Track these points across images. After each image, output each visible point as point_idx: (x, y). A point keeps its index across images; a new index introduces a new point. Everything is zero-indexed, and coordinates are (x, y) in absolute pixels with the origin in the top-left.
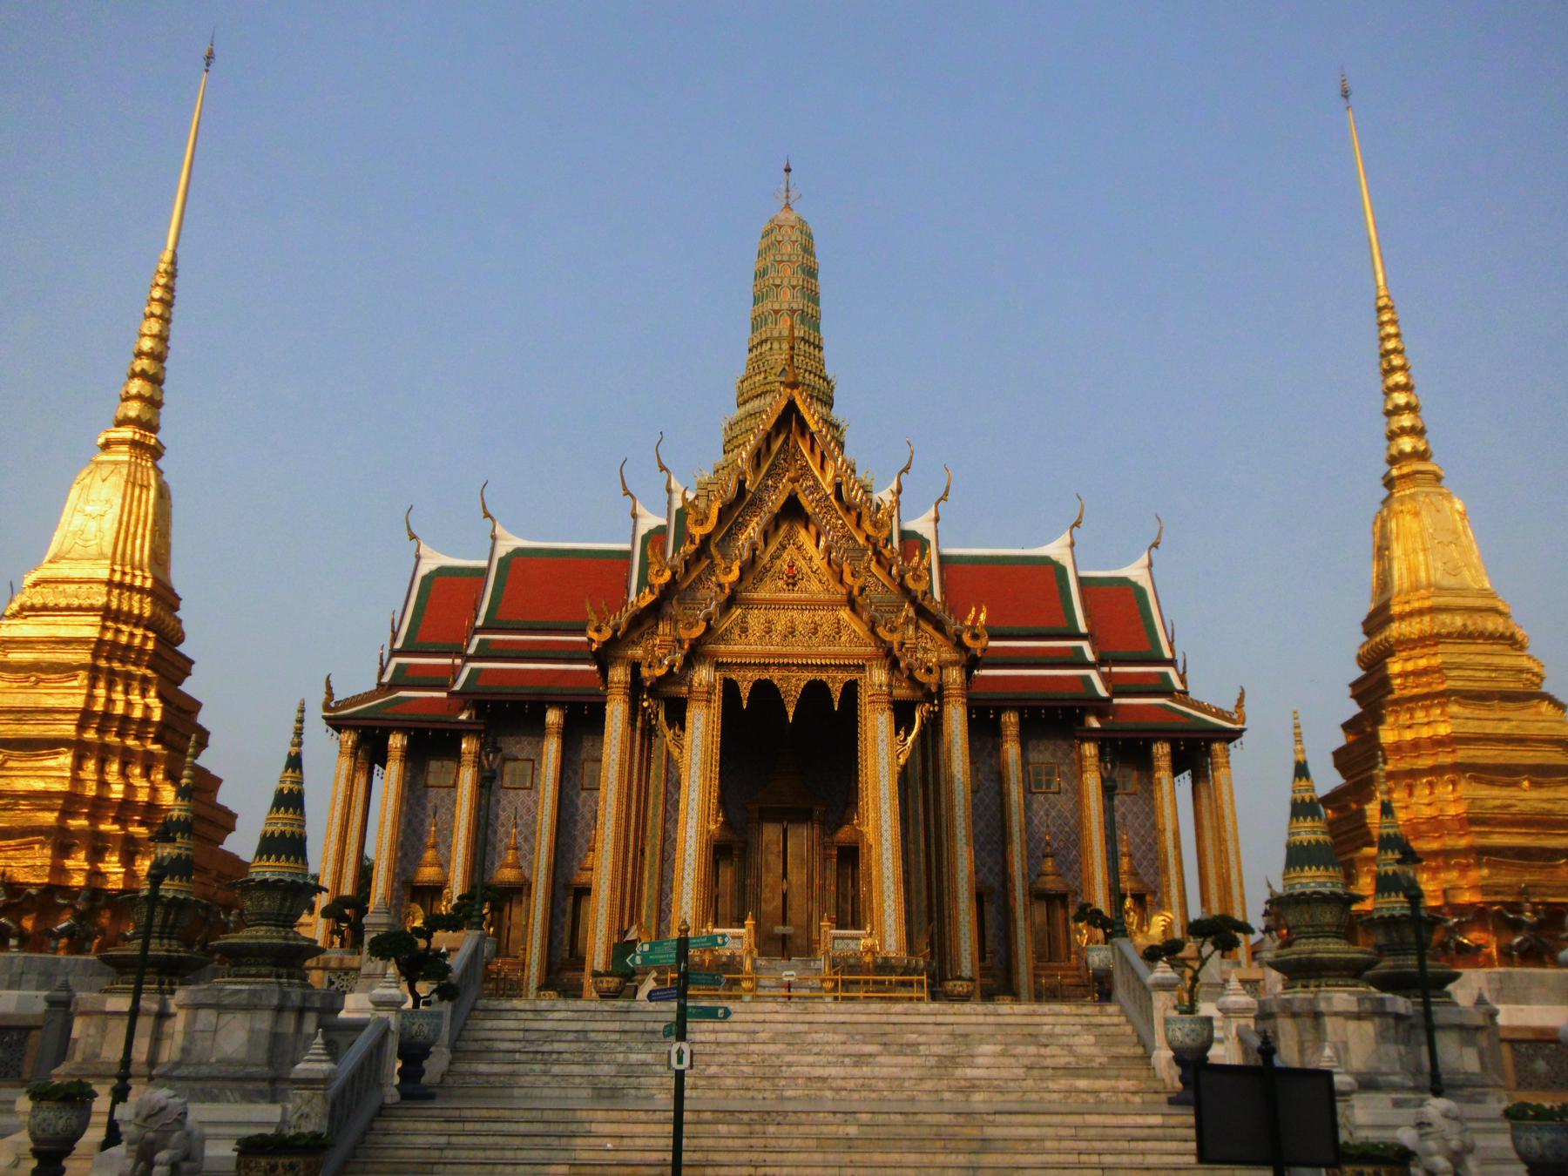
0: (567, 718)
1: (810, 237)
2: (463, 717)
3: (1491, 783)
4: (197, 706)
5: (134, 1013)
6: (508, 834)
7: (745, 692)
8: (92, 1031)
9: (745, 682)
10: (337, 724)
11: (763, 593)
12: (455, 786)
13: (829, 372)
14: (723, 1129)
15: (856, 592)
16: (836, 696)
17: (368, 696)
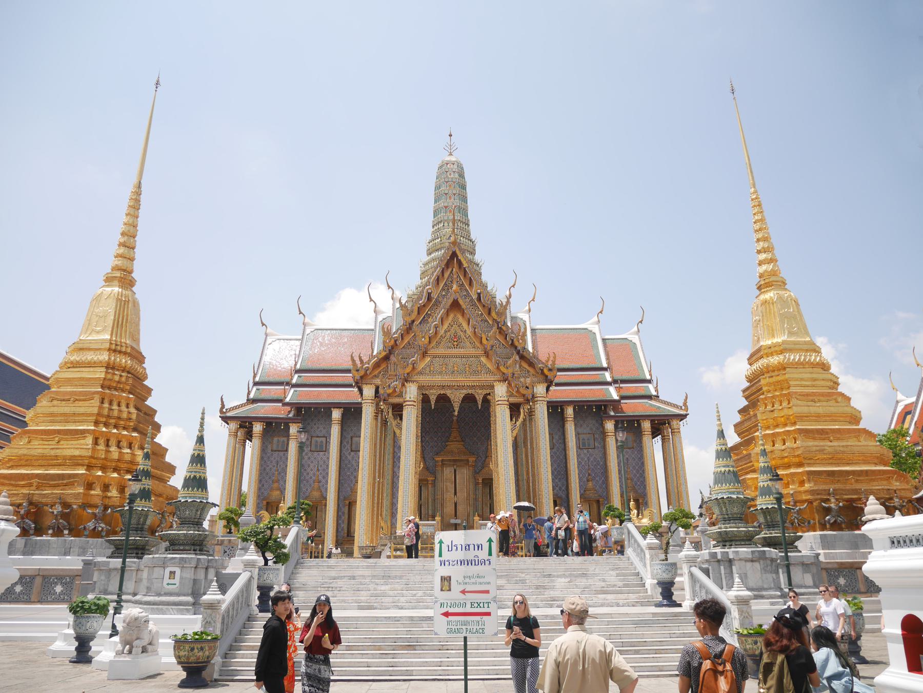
0: (343, 415)
1: (462, 168)
3: (814, 439)
4: (155, 412)
5: (123, 570)
7: (433, 399)
8: (103, 578)
10: (226, 419)
11: (441, 351)
12: (287, 450)
13: (473, 237)
15: (489, 348)
16: (480, 403)
17: (242, 405)
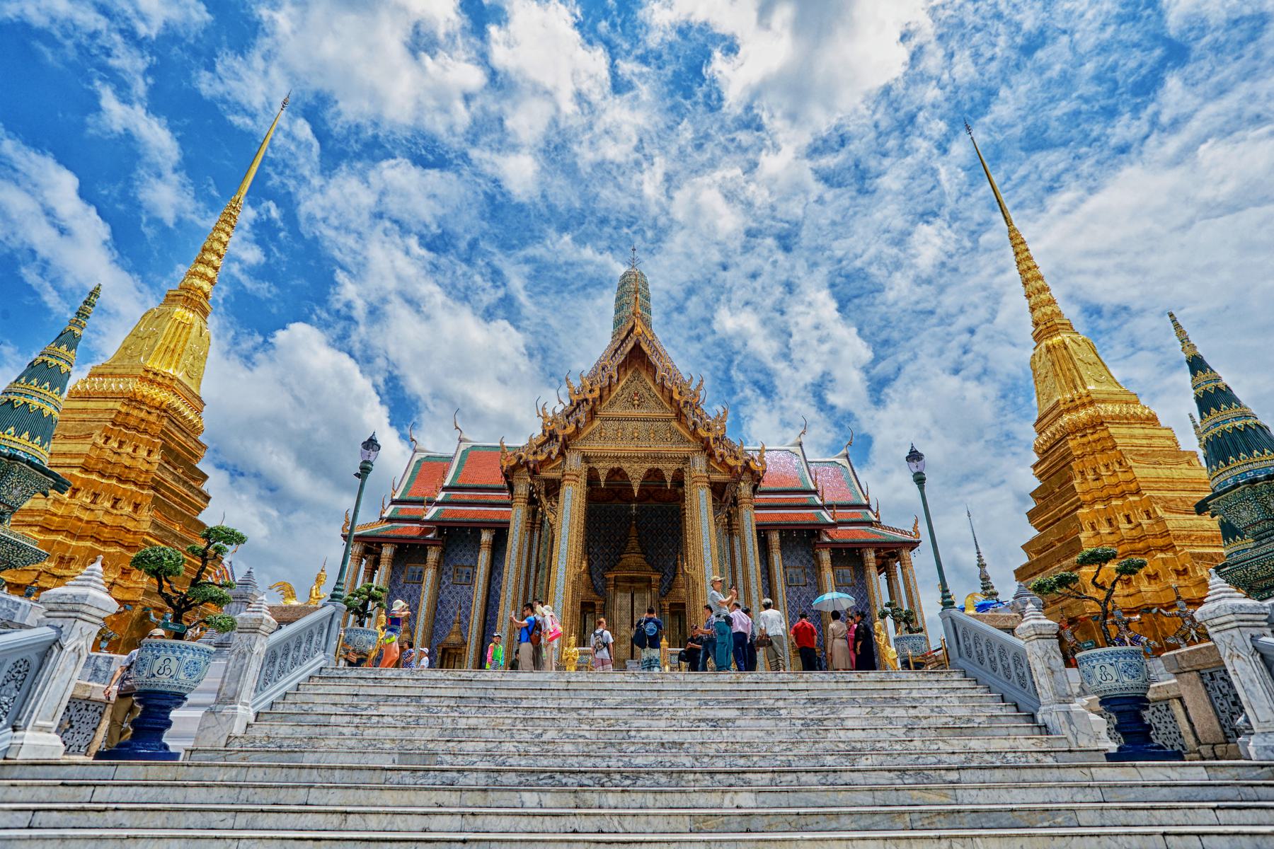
2: (430, 536)
6: (455, 613)
7: (603, 479)
9: (603, 469)
14: (530, 799)
